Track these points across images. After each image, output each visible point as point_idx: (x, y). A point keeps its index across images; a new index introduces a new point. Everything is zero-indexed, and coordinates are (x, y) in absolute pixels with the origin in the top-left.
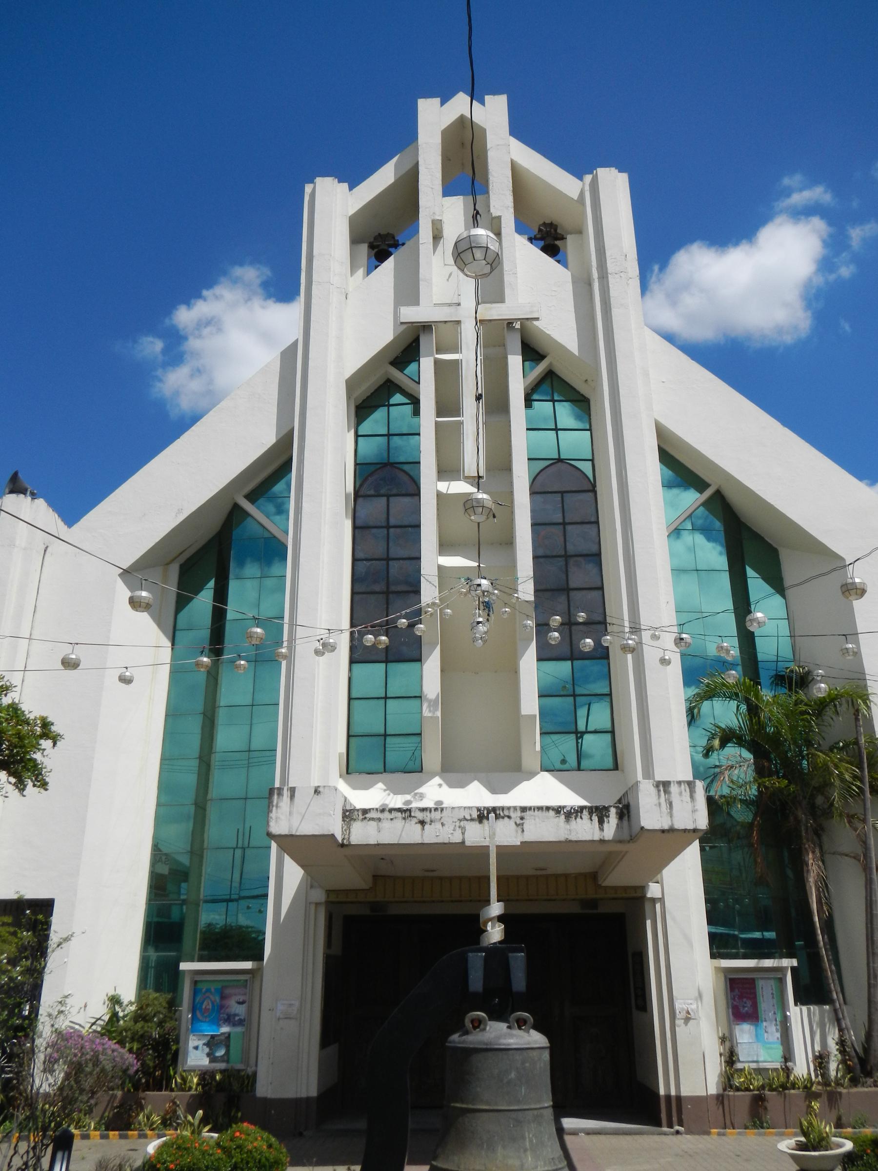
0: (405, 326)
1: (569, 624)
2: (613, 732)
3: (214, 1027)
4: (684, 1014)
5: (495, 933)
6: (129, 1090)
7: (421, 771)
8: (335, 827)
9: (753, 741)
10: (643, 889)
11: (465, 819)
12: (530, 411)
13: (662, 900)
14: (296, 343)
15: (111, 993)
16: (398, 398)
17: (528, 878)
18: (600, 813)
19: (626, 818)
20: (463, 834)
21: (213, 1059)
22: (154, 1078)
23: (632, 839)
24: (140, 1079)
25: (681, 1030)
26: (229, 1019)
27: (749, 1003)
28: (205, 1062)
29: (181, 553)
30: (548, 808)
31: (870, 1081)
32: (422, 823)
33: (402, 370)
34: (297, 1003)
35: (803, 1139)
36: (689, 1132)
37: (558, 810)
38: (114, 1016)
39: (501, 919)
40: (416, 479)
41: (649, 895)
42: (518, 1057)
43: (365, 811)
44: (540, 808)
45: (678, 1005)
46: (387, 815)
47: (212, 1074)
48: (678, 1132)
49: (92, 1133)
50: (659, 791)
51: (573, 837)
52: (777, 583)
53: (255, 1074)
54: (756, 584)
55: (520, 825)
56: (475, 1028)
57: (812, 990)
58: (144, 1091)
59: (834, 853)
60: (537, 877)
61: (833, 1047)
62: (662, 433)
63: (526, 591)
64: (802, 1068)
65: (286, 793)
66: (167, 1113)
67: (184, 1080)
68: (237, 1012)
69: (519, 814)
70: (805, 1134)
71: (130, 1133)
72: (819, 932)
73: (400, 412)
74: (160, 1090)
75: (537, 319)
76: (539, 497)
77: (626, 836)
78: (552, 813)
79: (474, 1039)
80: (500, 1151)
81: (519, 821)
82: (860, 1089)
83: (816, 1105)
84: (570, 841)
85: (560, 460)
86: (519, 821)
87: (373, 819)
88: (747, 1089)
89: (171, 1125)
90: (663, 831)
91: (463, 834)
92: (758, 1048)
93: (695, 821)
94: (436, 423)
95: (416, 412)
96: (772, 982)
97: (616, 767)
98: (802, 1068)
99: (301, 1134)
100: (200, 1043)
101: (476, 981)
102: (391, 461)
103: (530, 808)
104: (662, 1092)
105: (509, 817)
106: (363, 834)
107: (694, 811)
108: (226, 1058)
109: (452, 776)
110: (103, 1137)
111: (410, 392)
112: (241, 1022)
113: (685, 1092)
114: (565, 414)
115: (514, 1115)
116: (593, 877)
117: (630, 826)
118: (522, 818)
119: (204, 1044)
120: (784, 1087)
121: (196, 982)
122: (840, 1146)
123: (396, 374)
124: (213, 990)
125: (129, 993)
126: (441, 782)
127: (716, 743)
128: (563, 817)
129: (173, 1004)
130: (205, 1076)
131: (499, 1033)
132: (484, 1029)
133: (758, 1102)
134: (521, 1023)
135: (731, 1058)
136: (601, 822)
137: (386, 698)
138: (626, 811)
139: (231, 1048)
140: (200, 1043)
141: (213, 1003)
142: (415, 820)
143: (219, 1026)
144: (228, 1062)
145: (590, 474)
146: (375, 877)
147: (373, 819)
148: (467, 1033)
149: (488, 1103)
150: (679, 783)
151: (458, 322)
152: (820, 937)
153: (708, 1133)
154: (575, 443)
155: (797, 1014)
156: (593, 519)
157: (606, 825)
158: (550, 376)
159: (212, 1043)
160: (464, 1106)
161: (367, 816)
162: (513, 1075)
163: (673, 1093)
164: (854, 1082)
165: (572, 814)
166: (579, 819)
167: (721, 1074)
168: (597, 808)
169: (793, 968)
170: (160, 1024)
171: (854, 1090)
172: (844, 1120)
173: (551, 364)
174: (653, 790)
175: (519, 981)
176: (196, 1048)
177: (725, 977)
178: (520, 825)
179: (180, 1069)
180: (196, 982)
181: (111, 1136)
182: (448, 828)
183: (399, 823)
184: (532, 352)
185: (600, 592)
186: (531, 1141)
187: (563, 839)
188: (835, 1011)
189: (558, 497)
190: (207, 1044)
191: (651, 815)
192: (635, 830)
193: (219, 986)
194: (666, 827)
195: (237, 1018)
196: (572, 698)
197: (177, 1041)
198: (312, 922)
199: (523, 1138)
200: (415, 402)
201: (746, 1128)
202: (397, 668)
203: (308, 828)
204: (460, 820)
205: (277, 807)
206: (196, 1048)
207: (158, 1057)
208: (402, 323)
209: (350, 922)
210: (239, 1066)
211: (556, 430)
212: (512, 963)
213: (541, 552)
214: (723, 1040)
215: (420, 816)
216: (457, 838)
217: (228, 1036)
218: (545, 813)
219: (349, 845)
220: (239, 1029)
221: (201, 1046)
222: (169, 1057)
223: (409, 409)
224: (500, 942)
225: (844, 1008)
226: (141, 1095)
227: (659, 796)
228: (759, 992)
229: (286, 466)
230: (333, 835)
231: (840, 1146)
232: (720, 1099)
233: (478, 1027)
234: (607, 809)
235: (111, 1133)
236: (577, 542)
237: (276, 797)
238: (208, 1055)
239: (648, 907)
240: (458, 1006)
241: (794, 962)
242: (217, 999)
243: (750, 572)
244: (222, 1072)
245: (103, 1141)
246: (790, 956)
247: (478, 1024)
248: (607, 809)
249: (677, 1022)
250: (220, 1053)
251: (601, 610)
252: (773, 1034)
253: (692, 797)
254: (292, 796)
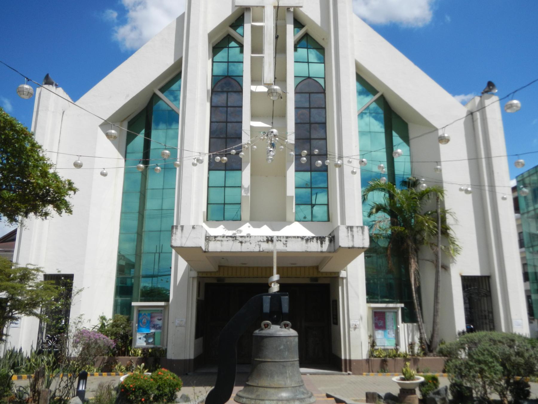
0: (237, 8)
1: (310, 155)
2: (328, 205)
4: (354, 326)
5: (275, 288)
6: (111, 356)
7: (241, 220)
8: (202, 244)
9: (391, 210)
10: (338, 273)
11: (261, 241)
12: (296, 53)
13: (346, 278)
14: (184, 14)
15: (101, 315)
16: (233, 44)
17: (287, 268)
18: (321, 239)
19: (333, 242)
20: (260, 247)
21: (148, 343)
22: (122, 351)
23: (335, 251)
24: (115, 351)
25: (352, 332)
26: (154, 327)
27: (382, 322)
28: (144, 344)
29: (128, 116)
30: (298, 237)
31: (432, 354)
32: (241, 242)
33: (235, 30)
34: (185, 320)
35: (403, 376)
36: (354, 374)
37: (302, 238)
38: (103, 325)
39: (278, 282)
40: (240, 83)
41: (341, 276)
42: (284, 340)
43: (215, 237)
44: (294, 237)
45: (352, 322)
46: (225, 239)
47: (147, 349)
48: (349, 374)
49: (95, 373)
50: (348, 230)
51: (309, 250)
52: (406, 139)
53: (166, 349)
54: (396, 139)
55: (285, 244)
56: (266, 327)
57: (410, 316)
58: (117, 356)
59: (423, 260)
60: (292, 267)
61: (417, 340)
62: (358, 66)
63: (291, 139)
64: (403, 348)
65: (179, 228)
66: (128, 365)
67: (135, 352)
69: (285, 239)
70: (404, 374)
71: (112, 373)
72: (414, 293)
73: (234, 51)
74: (125, 356)
75: (301, 7)
76: (299, 95)
77: (332, 250)
78: (300, 239)
79: (265, 332)
80: (276, 378)
81: (285, 242)
82: (427, 358)
83: (408, 364)
85: (309, 77)
86: (285, 242)
87: (219, 240)
88: (379, 357)
89: (130, 370)
90: (349, 248)
91: (260, 247)
92: (385, 341)
93: (363, 244)
94: (252, 57)
95: (242, 51)
96: (392, 314)
97: (329, 220)
98: (403, 348)
99: (187, 374)
100: (142, 336)
101: (266, 308)
102: (229, 75)
103: (290, 237)
104: (343, 358)
105: (280, 241)
106: (214, 247)
107: (363, 239)
108: (153, 343)
109: (254, 222)
110: (100, 375)
111: (239, 41)
112: (160, 328)
113: (353, 358)
114: (313, 55)
115: (282, 363)
116: (317, 268)
117: (334, 245)
118: (286, 241)
120: (395, 356)
121: (139, 311)
122: (418, 379)
123: (232, 31)
125: (109, 315)
126: (249, 225)
127: (374, 210)
128: (304, 241)
129: (129, 320)
130: (144, 350)
131: (276, 330)
132: (270, 328)
133: (384, 362)
134: (286, 326)
135: (373, 344)
136: (322, 243)
137: (225, 187)
138: (333, 239)
140: (142, 336)
143: (150, 329)
144: (154, 344)
145: (323, 85)
146: (220, 267)
147: (219, 240)
148: (262, 329)
149: (271, 359)
150: (357, 227)
151: (263, 7)
152: (414, 295)
153: (362, 374)
154: (316, 70)
155: (403, 327)
156: (323, 106)
157: (324, 245)
158: (306, 36)
159: (147, 336)
160: (261, 360)
161: (217, 239)
162: (282, 347)
163: (348, 358)
164: (425, 354)
165: (308, 240)
166: (312, 242)
167: (368, 351)
168: (320, 237)
169: (402, 308)
170: (124, 328)
171: (425, 358)
172: (420, 370)
173: (307, 30)
174: (345, 230)
175: (286, 308)
176: (140, 338)
177: (373, 311)
178: (285, 244)
179: (133, 347)
180: (139, 311)
182: (253, 245)
183: (231, 243)
184: (298, 24)
185: (325, 141)
186: (289, 374)
187: (304, 250)
188: (419, 326)
189: (307, 95)
190: (145, 337)
191: (344, 241)
192: (337, 247)
193: (150, 312)
194: (350, 246)
196: (310, 189)
197: (131, 335)
198: (191, 285)
199: (286, 373)
200: (241, 46)
201: (378, 372)
202: (230, 174)
203: (190, 243)
204: (258, 242)
205: (175, 234)
206: (140, 338)
207: (123, 342)
208: (236, 6)
209: (207, 285)
210: (159, 346)
211: (308, 62)
212: (282, 300)
213: (299, 121)
214: (370, 337)
215: (240, 239)
216: (257, 249)
218: (297, 239)
219: (208, 252)
220: (159, 331)
222: (128, 342)
223: (238, 49)
224: (277, 292)
225: (423, 325)
226: (116, 357)
227: (348, 232)
228: (387, 317)
229: (178, 76)
230: (201, 247)
231: (418, 379)
232: (368, 361)
233: (267, 327)
234: (324, 238)
235: (104, 373)
236: (316, 116)
237: (174, 230)
238: (145, 341)
239: (340, 281)
240: (259, 318)
241: (403, 305)
242: (149, 318)
243: (394, 134)
244: (152, 348)
245: (100, 377)
246: (401, 302)
247: (267, 326)
248: (324, 238)
249: (351, 329)
250: (151, 340)
251: (325, 149)
252: (392, 335)
253: (363, 233)
254: (182, 229)
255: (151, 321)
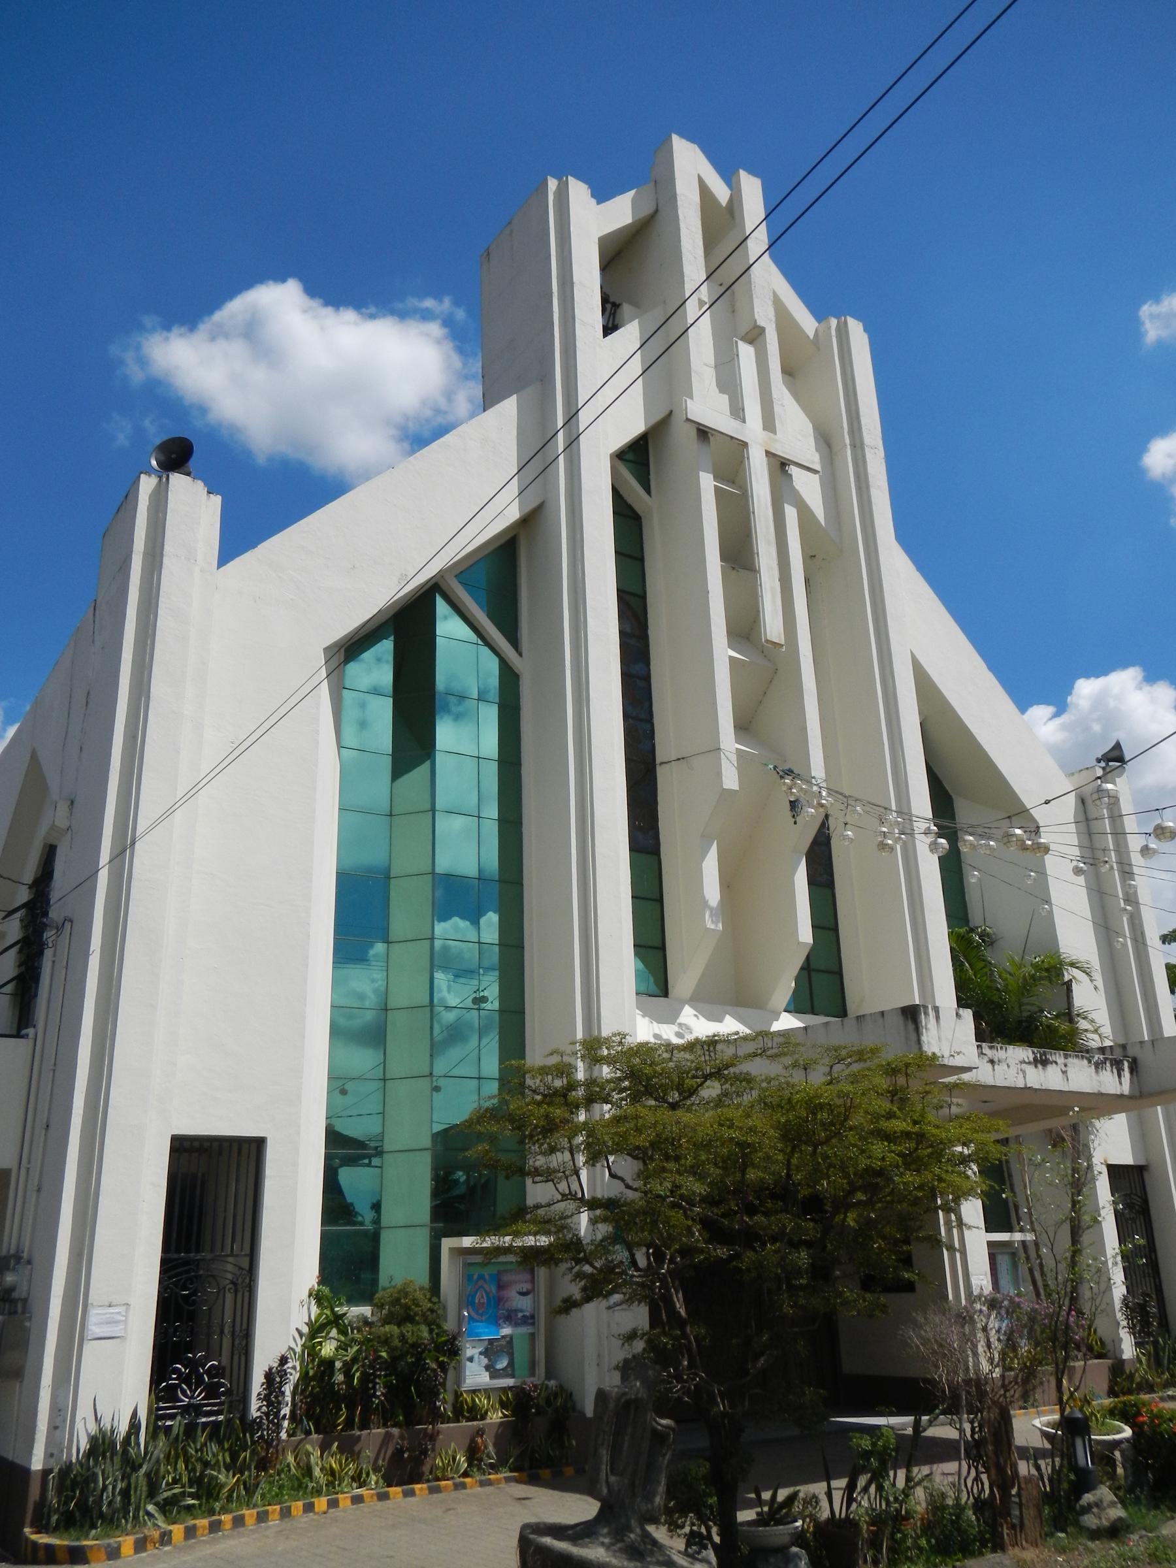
3: (493, 1328)
21: (494, 1374)
26: (510, 1317)
32: (992, 1062)
51: (1104, 1091)
68: (519, 1306)
84: (1102, 1094)
118: (1066, 1066)
119: (481, 1353)
124: (487, 1277)
139: (516, 1355)
141: (487, 1293)
142: (986, 1059)
143: (499, 1326)
159: (491, 1351)
181: (417, 1492)
190: (485, 1353)
195: (520, 1315)
217: (510, 1340)
220: (525, 1330)
221: (476, 1357)
238: (487, 1368)
250: (502, 1364)
254: (938, 1018)
255: (499, 1300)
